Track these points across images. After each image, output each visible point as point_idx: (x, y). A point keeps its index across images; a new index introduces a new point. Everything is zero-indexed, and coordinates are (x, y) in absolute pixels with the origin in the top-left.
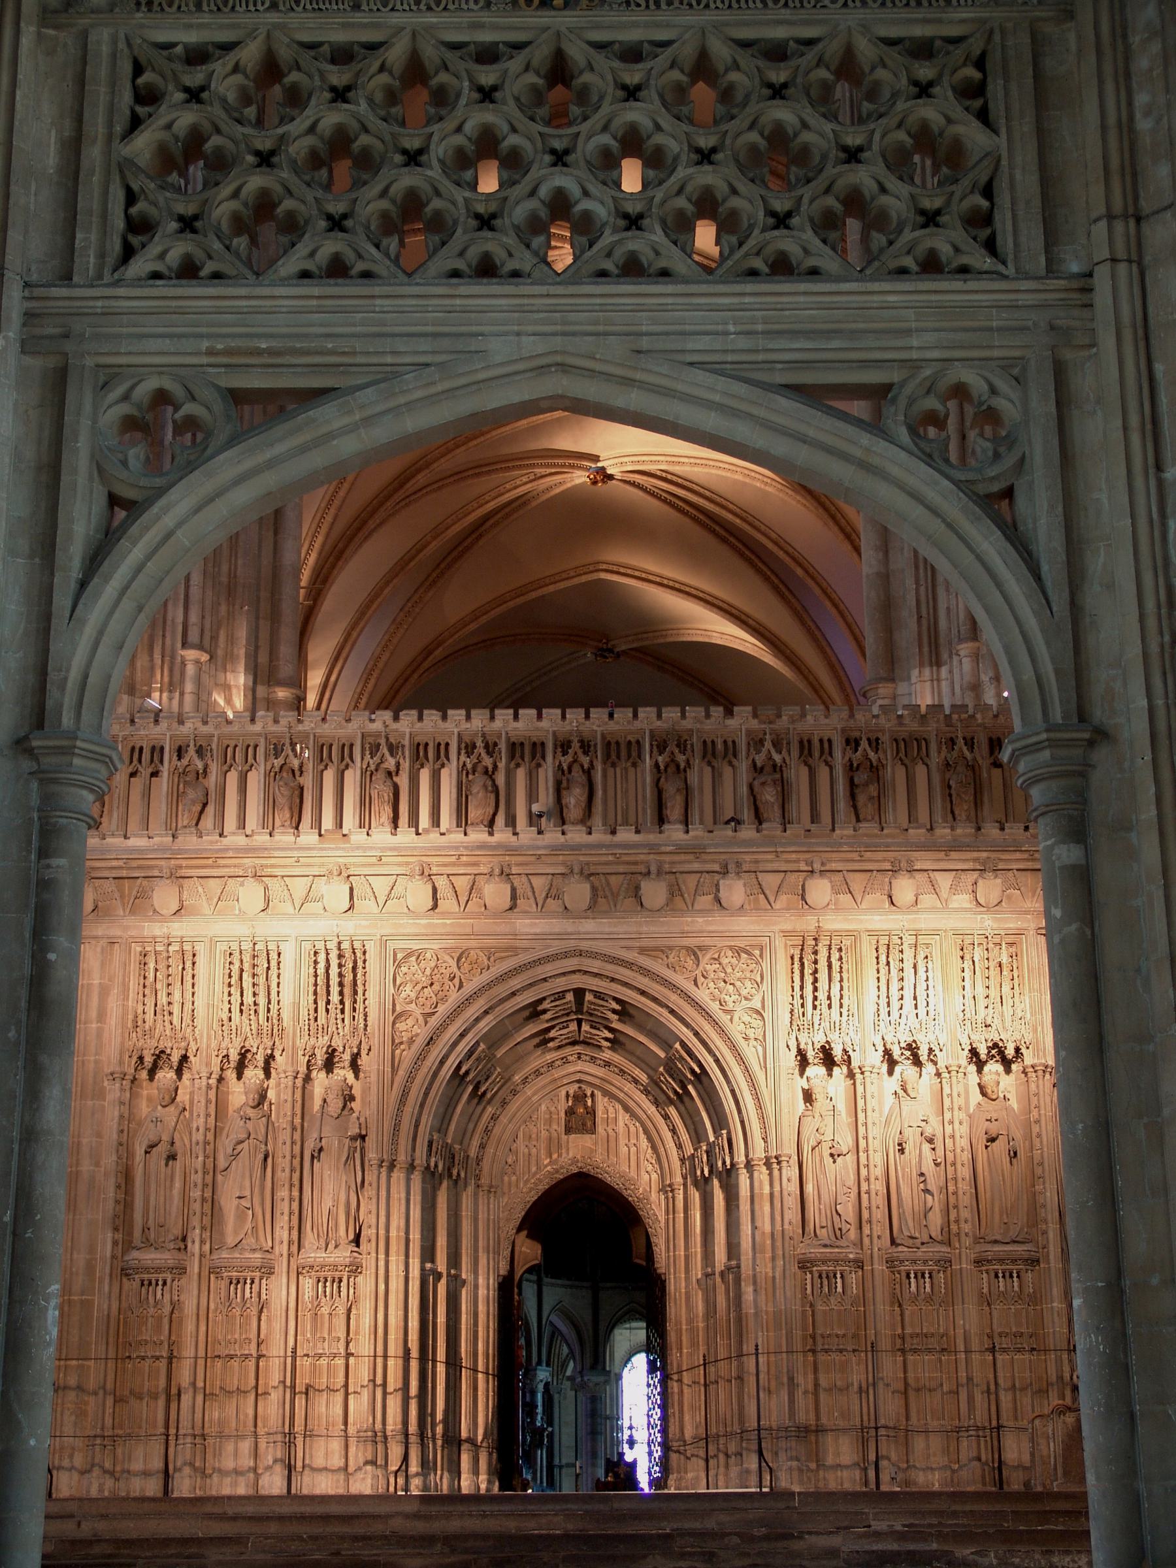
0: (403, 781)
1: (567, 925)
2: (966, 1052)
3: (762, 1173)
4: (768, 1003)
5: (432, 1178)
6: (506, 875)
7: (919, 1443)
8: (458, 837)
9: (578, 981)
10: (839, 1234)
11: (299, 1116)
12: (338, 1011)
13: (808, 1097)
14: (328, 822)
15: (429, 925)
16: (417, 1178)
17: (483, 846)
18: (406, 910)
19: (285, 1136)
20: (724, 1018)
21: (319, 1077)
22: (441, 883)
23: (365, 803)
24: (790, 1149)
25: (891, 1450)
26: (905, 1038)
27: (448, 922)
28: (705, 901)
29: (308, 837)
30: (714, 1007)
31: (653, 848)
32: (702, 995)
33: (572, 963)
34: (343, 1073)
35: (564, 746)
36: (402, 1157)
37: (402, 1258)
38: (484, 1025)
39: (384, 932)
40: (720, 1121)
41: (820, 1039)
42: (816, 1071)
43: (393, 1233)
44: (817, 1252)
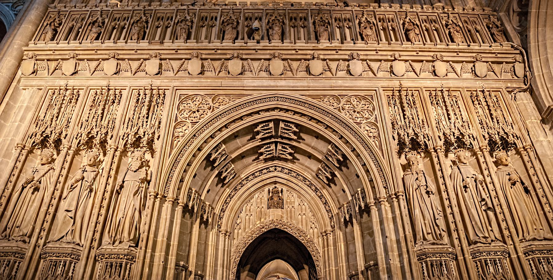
1: (272, 83)
2: (487, 142)
4: (379, 119)
11: (114, 170)
12: (145, 118)
15: (199, 82)
18: (188, 75)
27: (209, 80)
36: (170, 195)
37: (163, 253)
39: (175, 84)
43: (160, 239)
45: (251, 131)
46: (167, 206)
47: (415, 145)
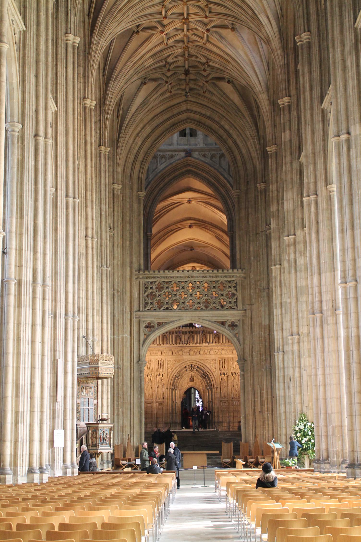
0: (168, 337)
3: (215, 389)
5: (173, 389)
6: (182, 350)
7: (235, 424)
8: (175, 345)
9: (192, 364)
10: (225, 397)
13: (222, 379)
14: (158, 343)
16: (171, 390)
17: (179, 347)
19: (154, 385)
20: (211, 369)
21: (158, 376)
22: (173, 351)
23: (163, 340)
24: (219, 386)
25: (231, 424)
26: (234, 372)
28: (208, 353)
29: (156, 345)
30: (209, 367)
31: (201, 346)
32: (208, 366)
33: (191, 361)
34: (161, 376)
35: (189, 332)
36: (169, 387)
38: (179, 370)
40: (210, 382)
41: (223, 372)
42: (223, 376)
44: (222, 400)
45: (186, 367)
46: (168, 390)
47: (224, 374)
